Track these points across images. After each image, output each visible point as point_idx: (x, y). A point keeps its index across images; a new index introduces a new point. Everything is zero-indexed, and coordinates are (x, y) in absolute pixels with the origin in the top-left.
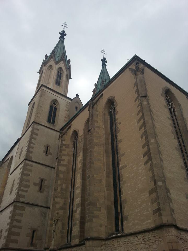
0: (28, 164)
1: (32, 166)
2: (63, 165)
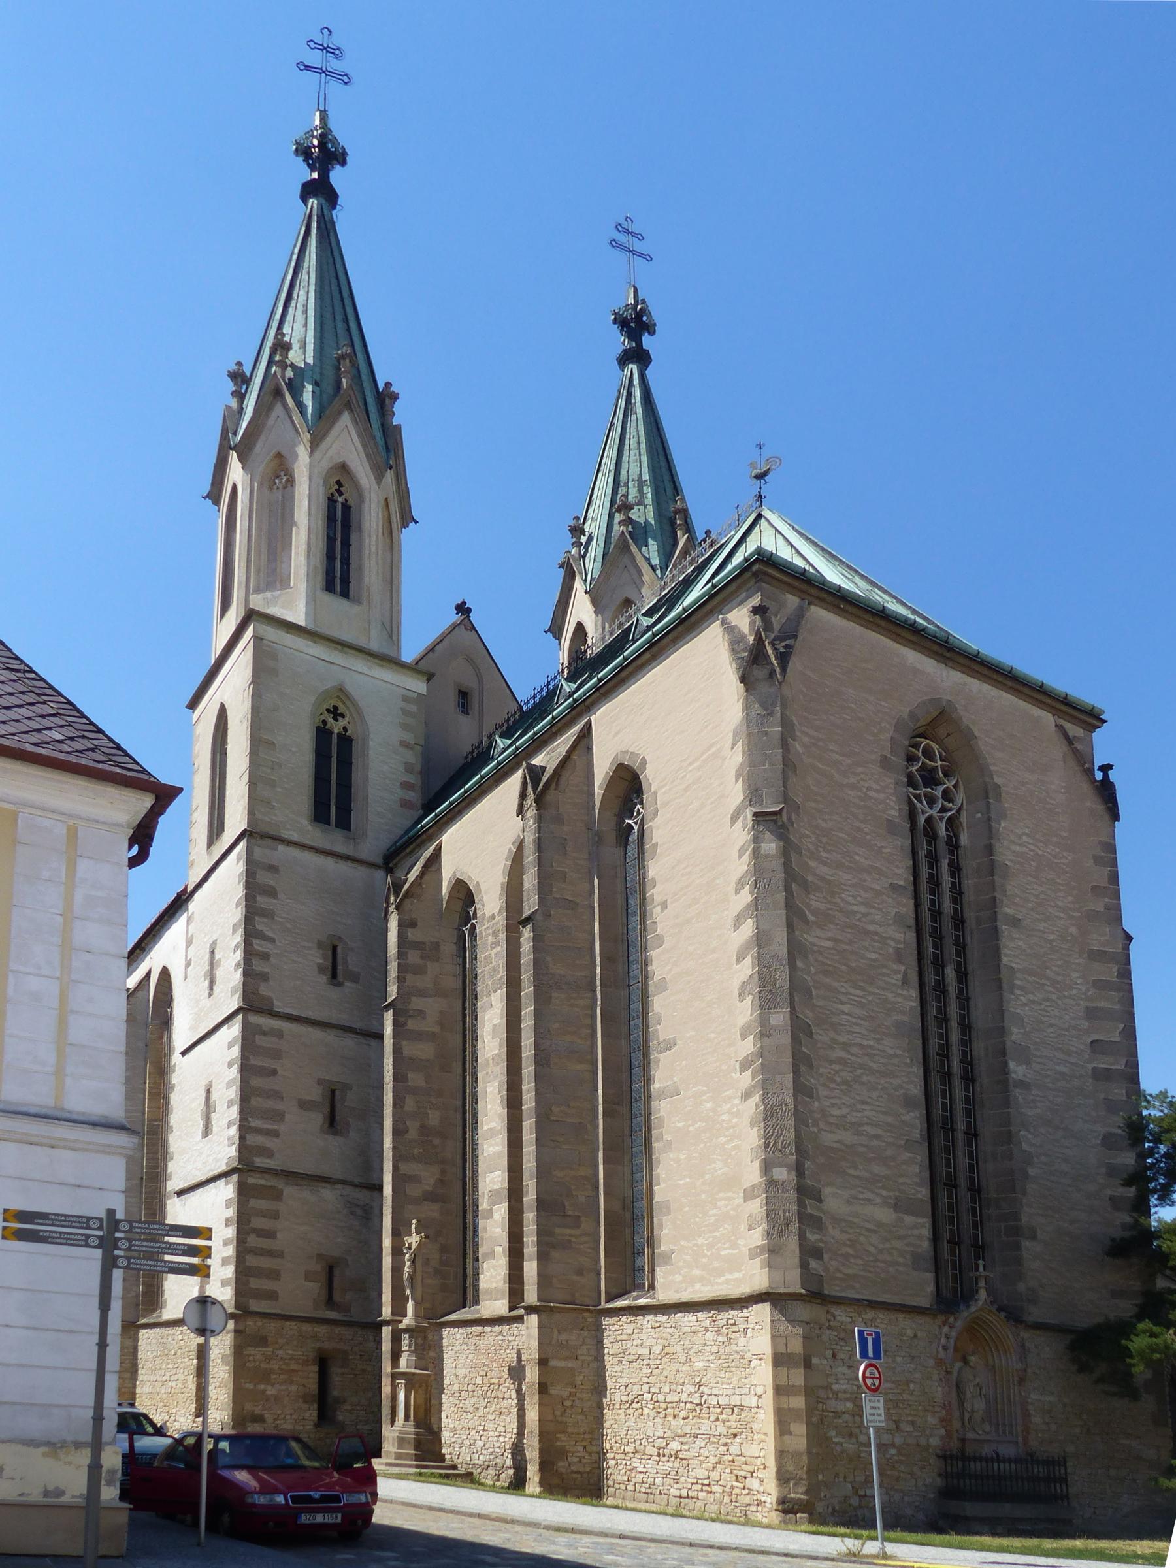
1: (279, 1034)
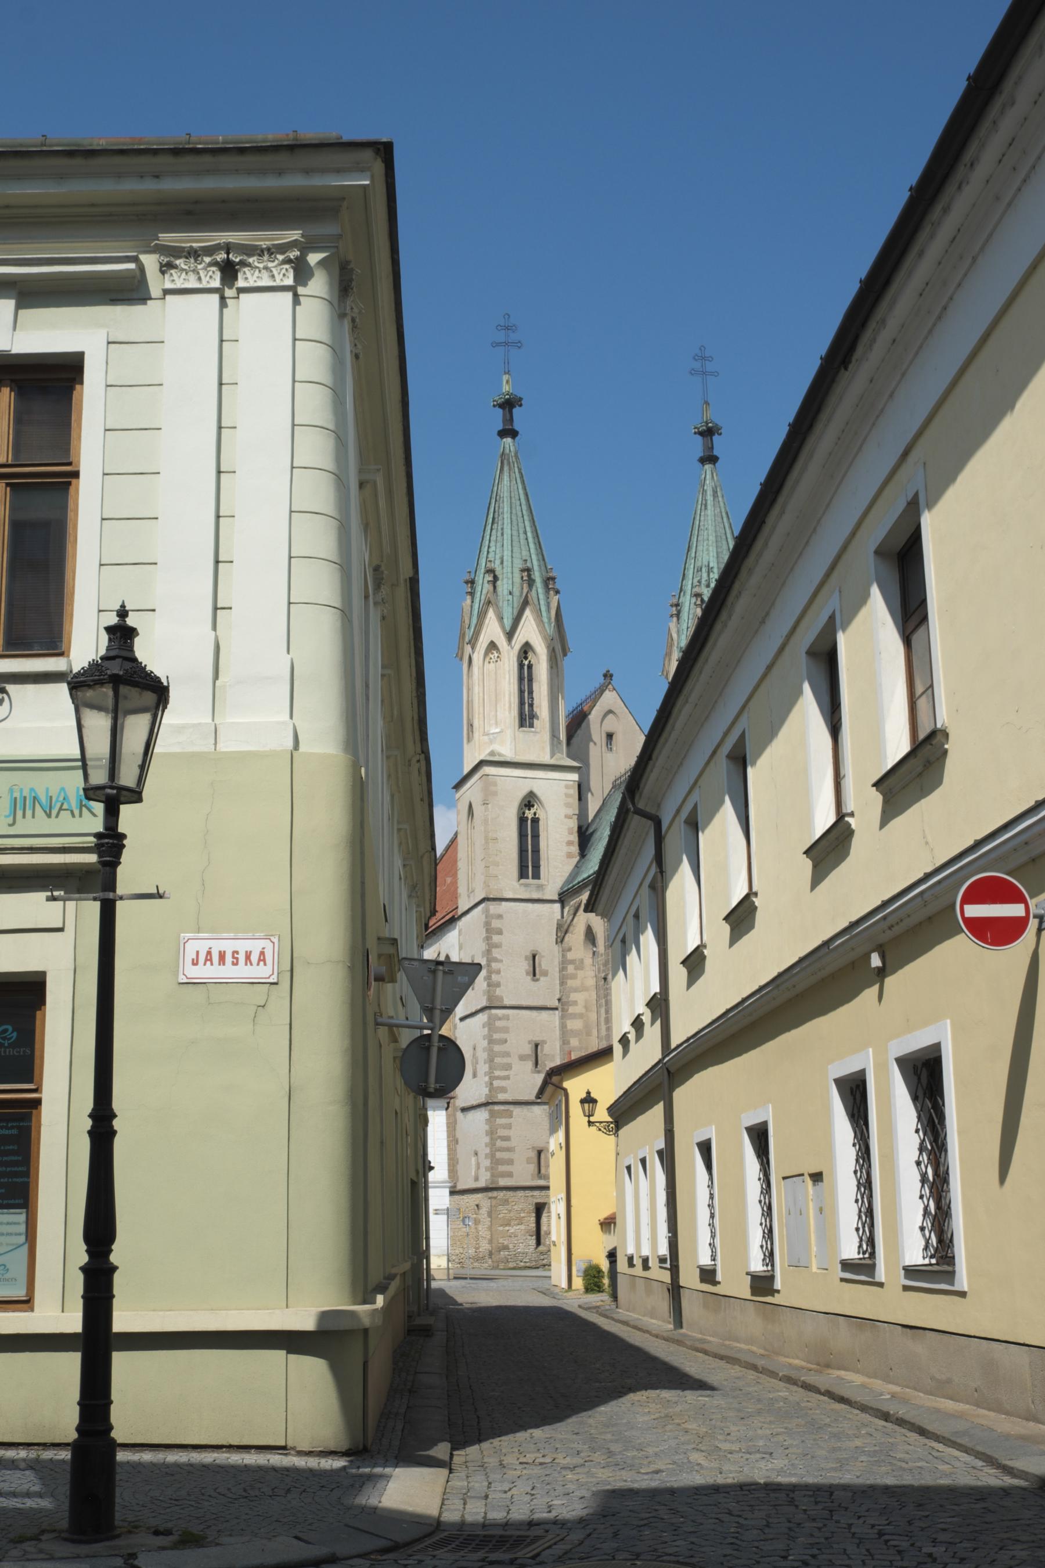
0: (496, 1015)
2: (574, 1016)
